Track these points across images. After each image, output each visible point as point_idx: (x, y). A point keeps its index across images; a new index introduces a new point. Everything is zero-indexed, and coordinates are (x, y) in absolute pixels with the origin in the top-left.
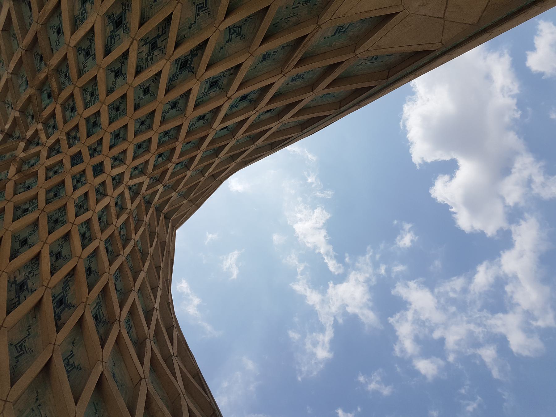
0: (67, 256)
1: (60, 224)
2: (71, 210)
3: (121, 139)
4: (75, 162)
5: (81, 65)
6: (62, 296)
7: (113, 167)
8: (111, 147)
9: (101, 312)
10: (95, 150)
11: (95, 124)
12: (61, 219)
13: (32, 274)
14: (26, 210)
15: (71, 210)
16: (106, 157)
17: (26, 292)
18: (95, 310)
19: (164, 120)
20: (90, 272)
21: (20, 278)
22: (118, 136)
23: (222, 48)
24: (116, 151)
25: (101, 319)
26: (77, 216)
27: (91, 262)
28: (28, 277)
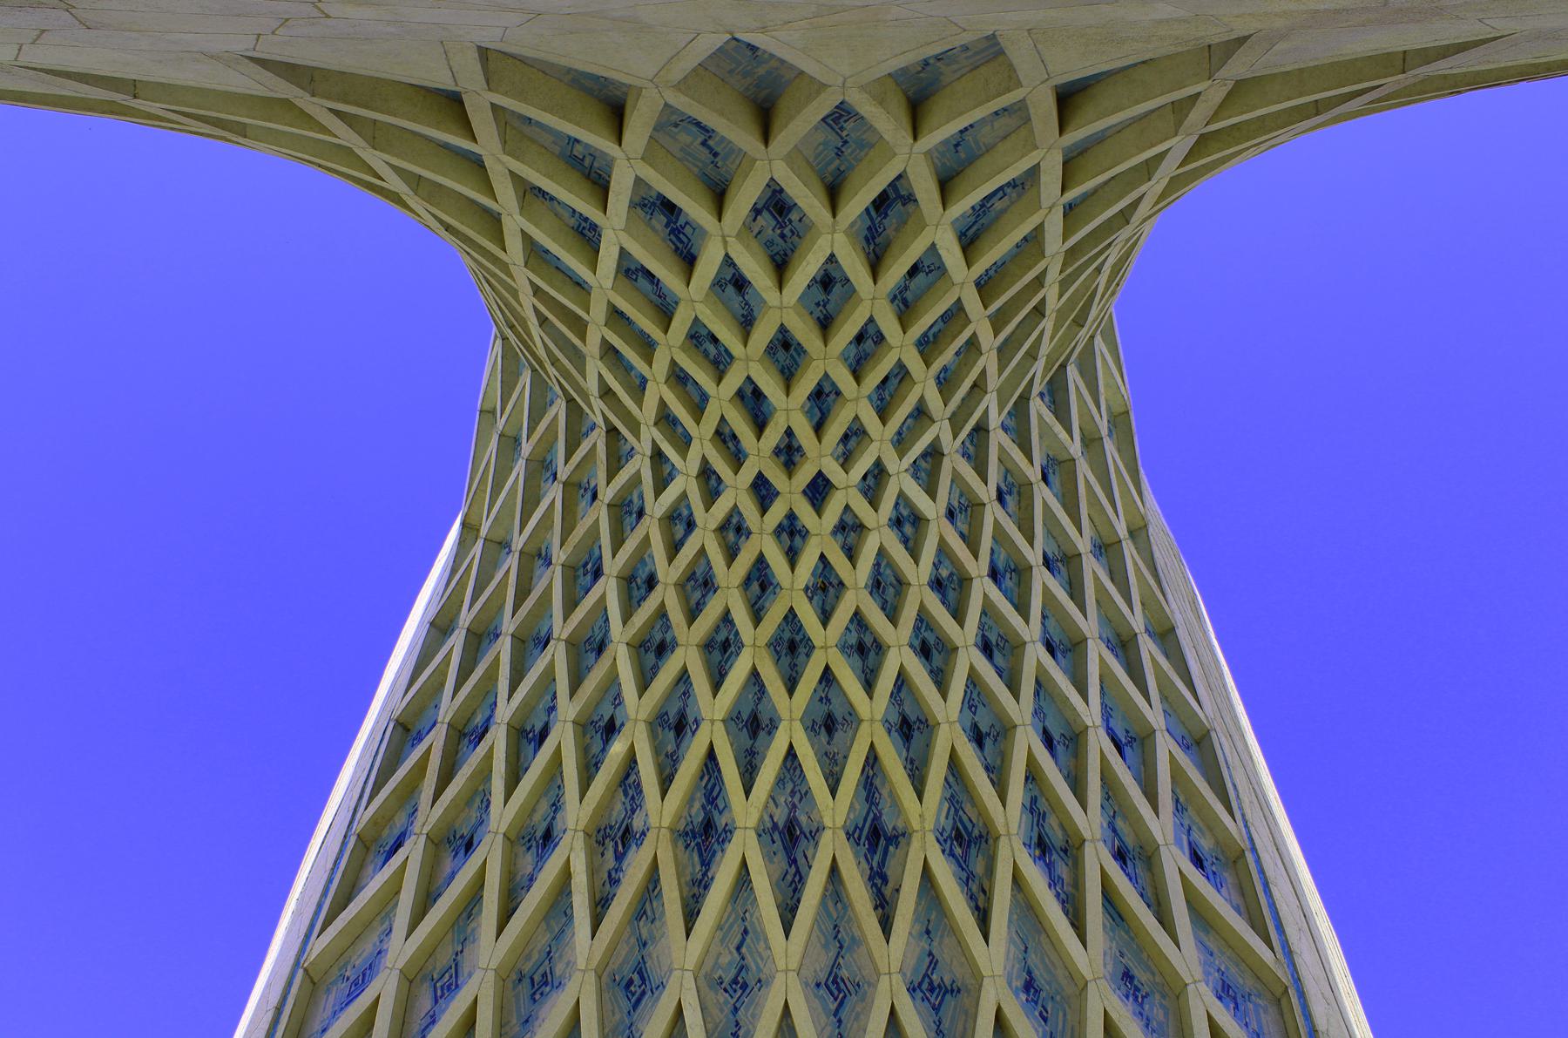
1: (802, 650)
2: (808, 616)
4: (764, 492)
5: (654, 298)
6: (876, 818)
9: (965, 819)
11: (758, 394)
12: (798, 638)
13: (798, 796)
14: (726, 645)
15: (808, 616)
16: (820, 456)
17: (803, 842)
18: (951, 821)
20: (910, 727)
21: (781, 816)
22: (823, 399)
23: (957, 145)
24: (835, 430)
25: (969, 834)
26: (825, 617)
27: (900, 703)
28: (794, 806)
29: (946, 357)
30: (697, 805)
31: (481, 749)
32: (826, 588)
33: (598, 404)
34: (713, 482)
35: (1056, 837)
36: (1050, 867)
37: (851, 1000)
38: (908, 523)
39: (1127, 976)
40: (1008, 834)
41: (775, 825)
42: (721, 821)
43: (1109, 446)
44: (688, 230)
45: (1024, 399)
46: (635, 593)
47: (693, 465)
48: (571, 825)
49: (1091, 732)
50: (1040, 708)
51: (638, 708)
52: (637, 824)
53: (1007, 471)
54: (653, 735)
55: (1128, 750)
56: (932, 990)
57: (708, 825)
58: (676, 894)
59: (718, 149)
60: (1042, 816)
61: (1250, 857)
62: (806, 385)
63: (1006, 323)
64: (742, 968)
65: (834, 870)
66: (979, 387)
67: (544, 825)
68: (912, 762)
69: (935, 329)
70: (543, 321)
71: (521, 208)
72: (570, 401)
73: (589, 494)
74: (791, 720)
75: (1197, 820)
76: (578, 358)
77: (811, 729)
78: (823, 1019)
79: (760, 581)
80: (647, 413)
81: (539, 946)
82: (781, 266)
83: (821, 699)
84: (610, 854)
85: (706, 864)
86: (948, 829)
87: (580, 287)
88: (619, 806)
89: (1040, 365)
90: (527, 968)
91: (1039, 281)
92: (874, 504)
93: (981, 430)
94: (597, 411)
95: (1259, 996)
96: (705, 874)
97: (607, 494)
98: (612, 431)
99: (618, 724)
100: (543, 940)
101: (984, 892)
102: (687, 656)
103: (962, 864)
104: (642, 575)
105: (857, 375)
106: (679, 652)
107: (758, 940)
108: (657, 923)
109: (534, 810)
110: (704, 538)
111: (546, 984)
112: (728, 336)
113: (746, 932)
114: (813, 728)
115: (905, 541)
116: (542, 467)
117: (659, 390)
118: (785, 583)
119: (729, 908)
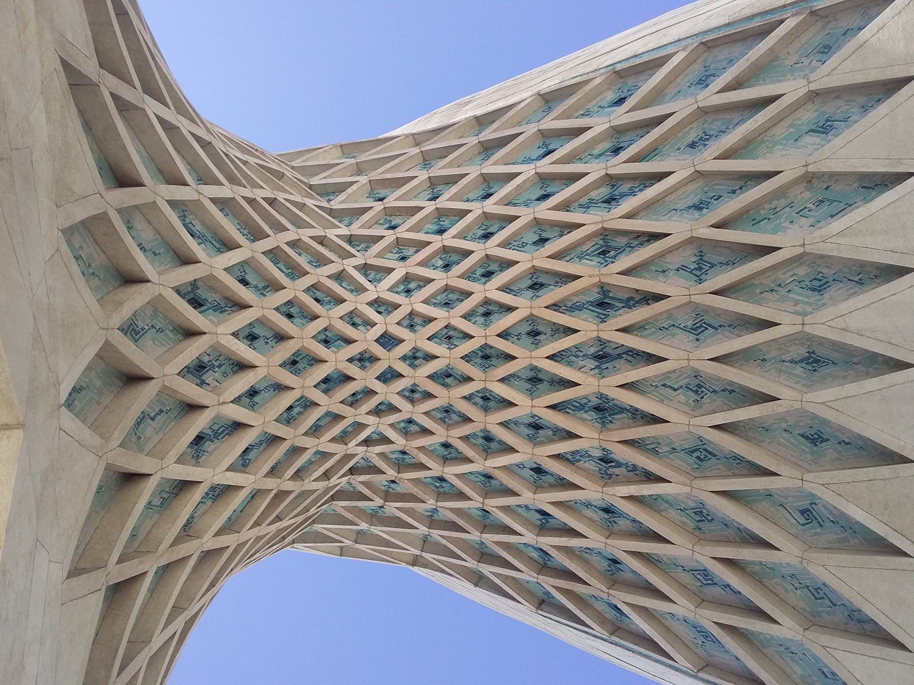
0: (530, 322)
1: (488, 352)
2: (466, 347)
3: (327, 333)
4: (389, 376)
5: (262, 447)
7: (371, 324)
8: (349, 341)
9: (592, 249)
10: (360, 360)
11: (326, 380)
12: (480, 354)
14: (485, 399)
15: (466, 347)
16: (366, 340)
19: (268, 286)
20: (536, 284)
21: (592, 364)
23: (155, 254)
24: (350, 332)
25: (602, 246)
27: (521, 290)
29: (302, 261)
30: (585, 416)
31: (553, 553)
32: (449, 336)
33: (334, 480)
34: (383, 407)
35: (604, 192)
36: (623, 195)
37: (707, 319)
38: (409, 285)
39: (693, 145)
40: (602, 222)
41: (596, 367)
42: (595, 401)
43: (363, 158)
44: (215, 427)
45: (330, 212)
46: (453, 455)
47: (371, 420)
48: (599, 496)
49: (539, 171)
50: (524, 202)
51: (527, 453)
52: (598, 453)
53: (376, 223)
54: (542, 443)
55: (551, 147)
56: (700, 269)
57: (597, 409)
58: (641, 429)
59: (157, 410)
60: (591, 201)
61: (619, 67)
62: (320, 350)
63: (279, 223)
64: (687, 387)
65: (624, 330)
66: (321, 240)
67: (600, 513)
68: (557, 282)
69: (284, 269)
70: (278, 519)
71: (198, 538)
72: (333, 498)
73: (392, 485)
74: (531, 357)
75: (594, 102)
76: (304, 495)
77: (537, 345)
78: (720, 336)
79: (444, 377)
80: (339, 450)
81: (677, 516)
82: (242, 366)
83: (519, 339)
84: (617, 471)
85: (622, 410)
86: (599, 259)
87: (255, 495)
88: (587, 465)
89: (309, 202)
90: (691, 524)
91: (251, 201)
92: (397, 306)
93: (350, 239)
94: (339, 481)
95: (706, 60)
96: (628, 411)
97: (391, 473)
98: (352, 471)
99: (536, 466)
100: (673, 514)
101: (638, 237)
102: (492, 422)
103: (620, 251)
104: (442, 451)
105: (315, 317)
106: (490, 427)
107: (670, 377)
108: (660, 441)
109: (590, 519)
110: (418, 412)
111: (701, 512)
112: (288, 399)
113: (664, 385)
114: (537, 344)
115: (420, 287)
116: (375, 517)
117: (324, 443)
118: (446, 362)
119: (650, 396)
